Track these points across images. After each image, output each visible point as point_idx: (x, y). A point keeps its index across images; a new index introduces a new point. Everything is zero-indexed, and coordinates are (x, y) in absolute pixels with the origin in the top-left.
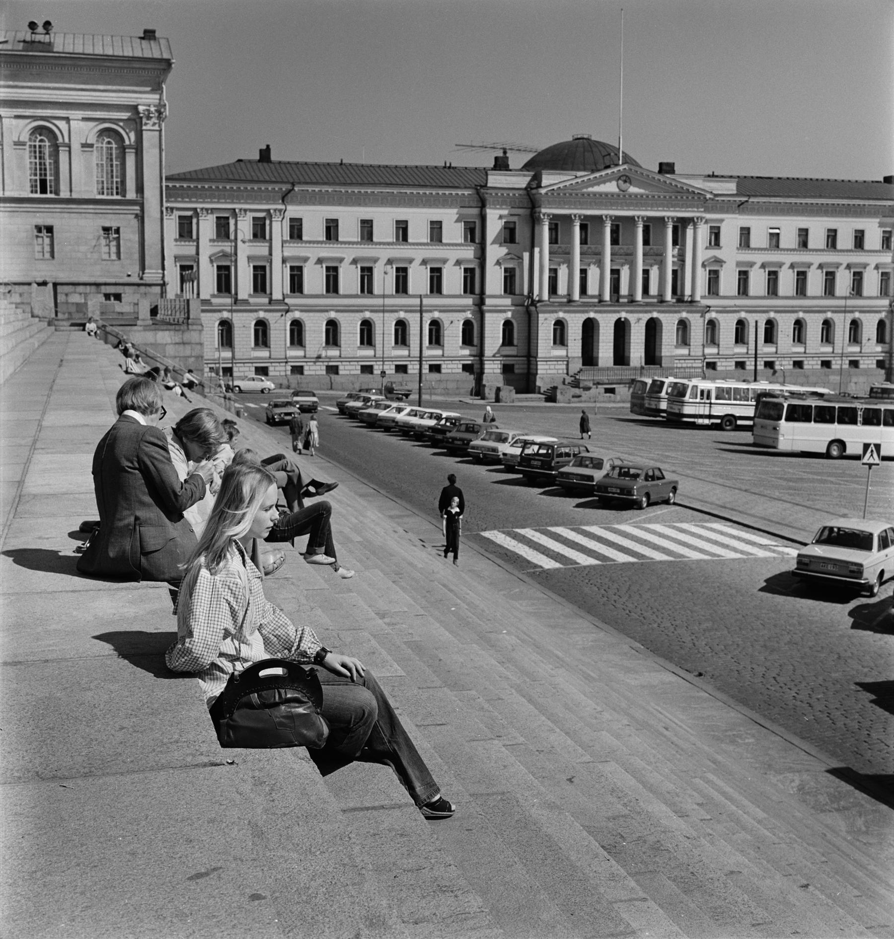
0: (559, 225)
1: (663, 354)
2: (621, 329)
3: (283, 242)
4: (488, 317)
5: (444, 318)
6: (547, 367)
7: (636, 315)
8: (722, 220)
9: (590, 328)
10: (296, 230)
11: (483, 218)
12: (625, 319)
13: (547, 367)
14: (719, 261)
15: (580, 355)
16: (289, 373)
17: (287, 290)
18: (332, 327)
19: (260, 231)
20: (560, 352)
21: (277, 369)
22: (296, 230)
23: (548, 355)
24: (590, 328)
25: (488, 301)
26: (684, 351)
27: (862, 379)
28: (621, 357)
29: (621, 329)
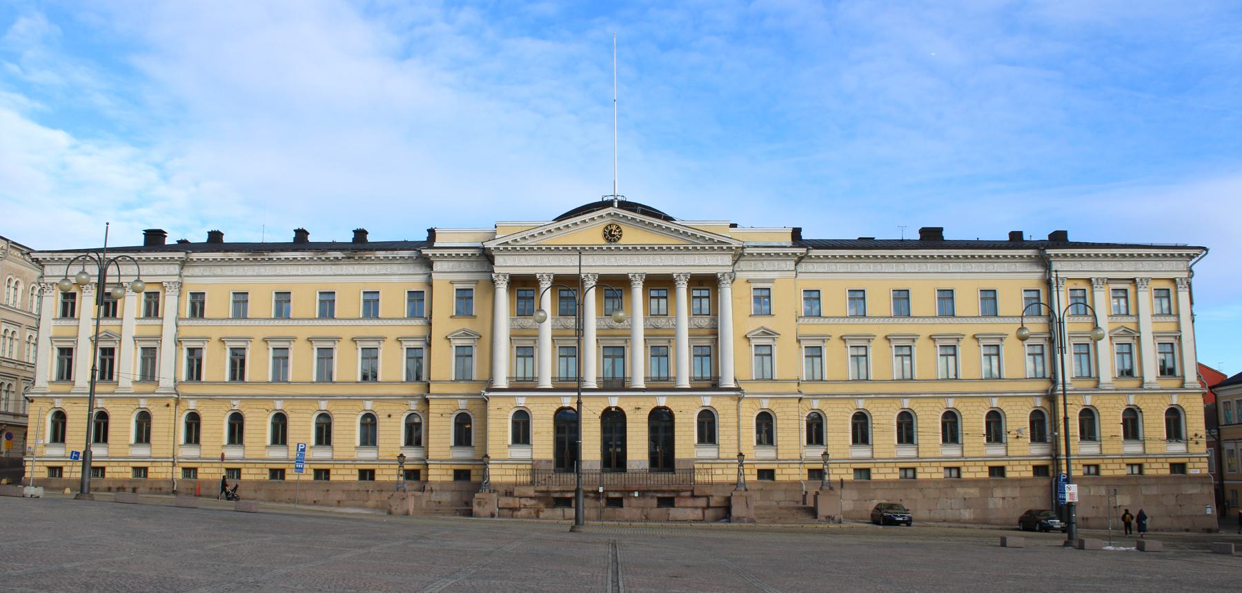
1: (677, 456)
2: (614, 422)
3: (178, 318)
5: (381, 411)
6: (503, 472)
7: (634, 403)
9: (567, 424)
10: (198, 306)
11: (430, 284)
12: (617, 408)
13: (503, 472)
14: (767, 333)
15: (551, 456)
17: (183, 376)
18: (280, 421)
19: (152, 307)
20: (521, 452)
21: (158, 470)
22: (198, 306)
23: (502, 457)
24: (567, 424)
25: (433, 389)
26: (708, 452)
27: (1009, 492)
29: (614, 422)
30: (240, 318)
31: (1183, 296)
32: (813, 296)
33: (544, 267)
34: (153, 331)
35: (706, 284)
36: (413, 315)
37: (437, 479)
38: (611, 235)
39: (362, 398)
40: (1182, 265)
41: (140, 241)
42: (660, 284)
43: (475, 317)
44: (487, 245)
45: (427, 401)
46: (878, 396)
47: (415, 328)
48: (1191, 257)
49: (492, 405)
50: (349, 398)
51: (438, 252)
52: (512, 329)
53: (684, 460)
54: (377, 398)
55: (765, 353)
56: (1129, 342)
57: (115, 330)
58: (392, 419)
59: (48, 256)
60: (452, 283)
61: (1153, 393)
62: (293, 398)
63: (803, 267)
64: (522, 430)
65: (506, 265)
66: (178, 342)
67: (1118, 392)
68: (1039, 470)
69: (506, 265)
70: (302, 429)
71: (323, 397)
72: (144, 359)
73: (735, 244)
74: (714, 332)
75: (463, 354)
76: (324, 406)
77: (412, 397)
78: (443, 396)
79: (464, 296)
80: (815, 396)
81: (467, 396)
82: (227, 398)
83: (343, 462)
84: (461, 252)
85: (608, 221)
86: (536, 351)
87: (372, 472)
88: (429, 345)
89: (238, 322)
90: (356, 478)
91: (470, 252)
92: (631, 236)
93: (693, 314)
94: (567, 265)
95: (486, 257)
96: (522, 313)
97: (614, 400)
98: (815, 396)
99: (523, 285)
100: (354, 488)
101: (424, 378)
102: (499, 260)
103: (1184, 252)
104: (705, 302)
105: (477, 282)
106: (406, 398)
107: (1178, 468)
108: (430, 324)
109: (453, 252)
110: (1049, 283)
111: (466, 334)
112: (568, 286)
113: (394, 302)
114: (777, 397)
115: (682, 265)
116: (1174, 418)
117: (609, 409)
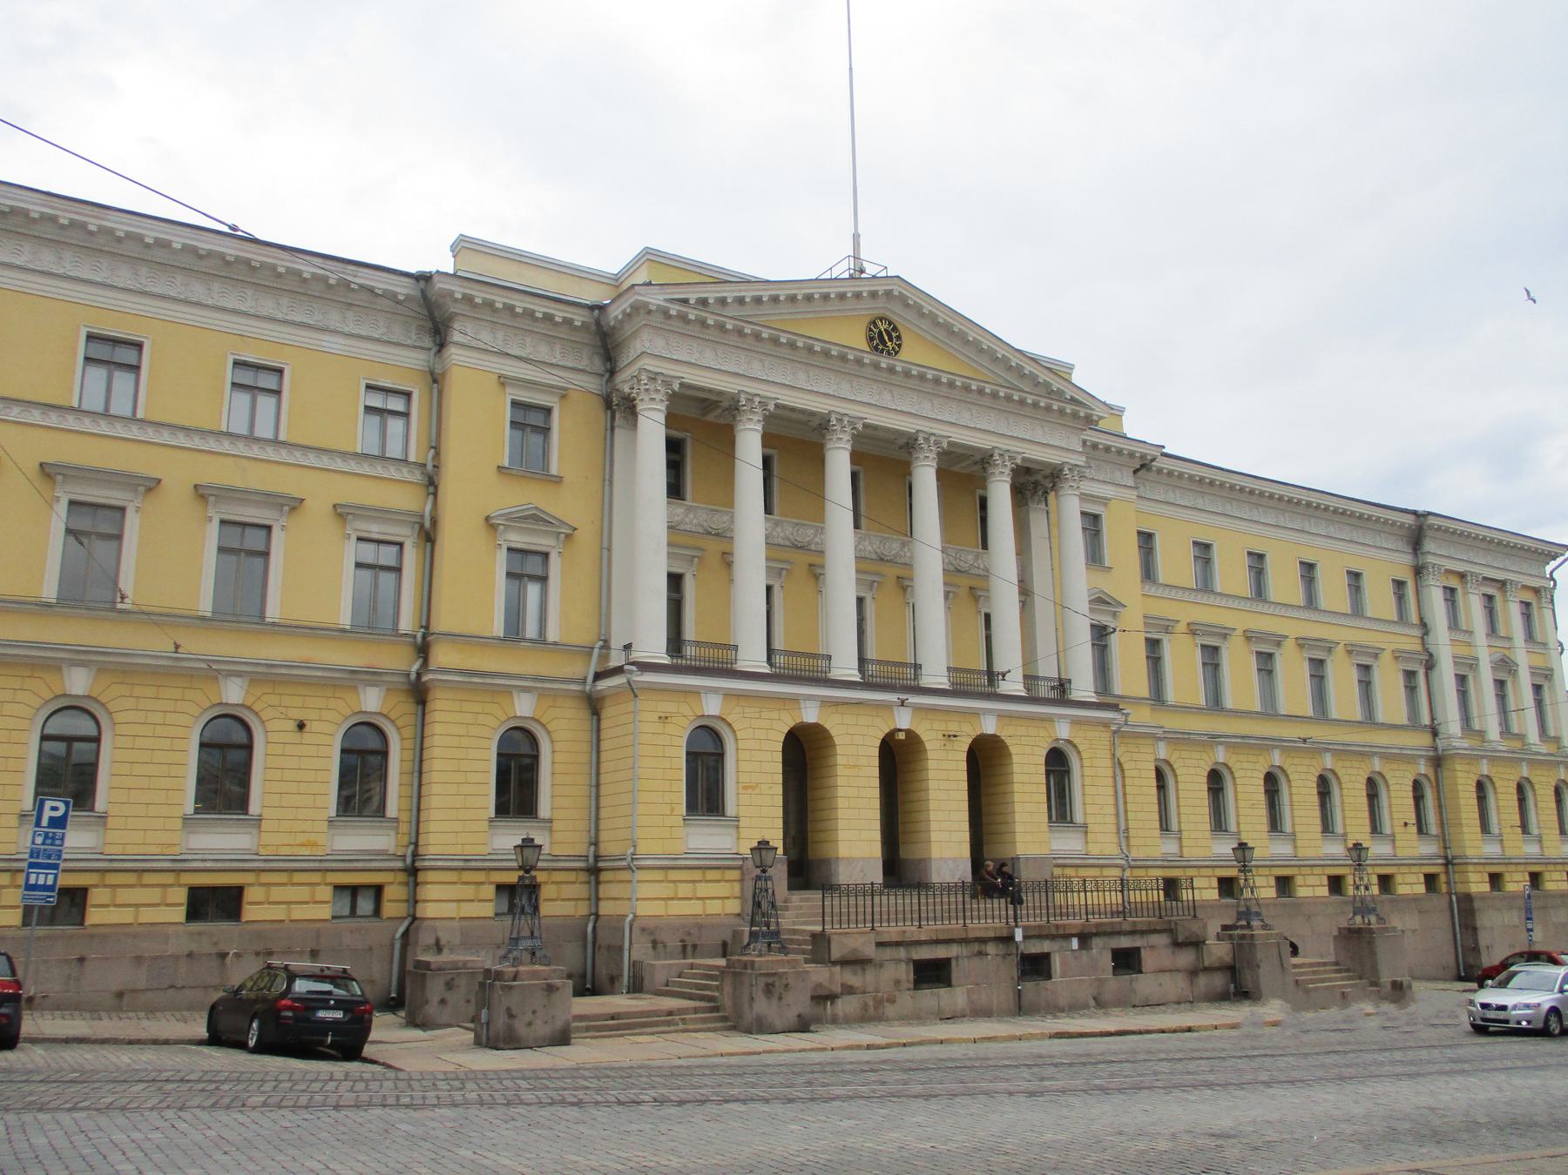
4: (442, 707)
12: (909, 732)
20: (709, 839)
25: (443, 656)
26: (1066, 843)
28: (899, 868)
33: (761, 383)
37: (449, 910)
39: (213, 672)
43: (558, 480)
45: (419, 694)
50: (175, 672)
53: (1038, 861)
54: (265, 676)
58: (307, 737)
60: (503, 381)
68: (1430, 880)
71: (81, 657)
77: (372, 676)
81: (540, 686)
87: (236, 893)
88: (428, 536)
90: (179, 914)
100: (186, 946)
105: (563, 394)
106: (355, 678)
108: (432, 484)
111: (536, 519)
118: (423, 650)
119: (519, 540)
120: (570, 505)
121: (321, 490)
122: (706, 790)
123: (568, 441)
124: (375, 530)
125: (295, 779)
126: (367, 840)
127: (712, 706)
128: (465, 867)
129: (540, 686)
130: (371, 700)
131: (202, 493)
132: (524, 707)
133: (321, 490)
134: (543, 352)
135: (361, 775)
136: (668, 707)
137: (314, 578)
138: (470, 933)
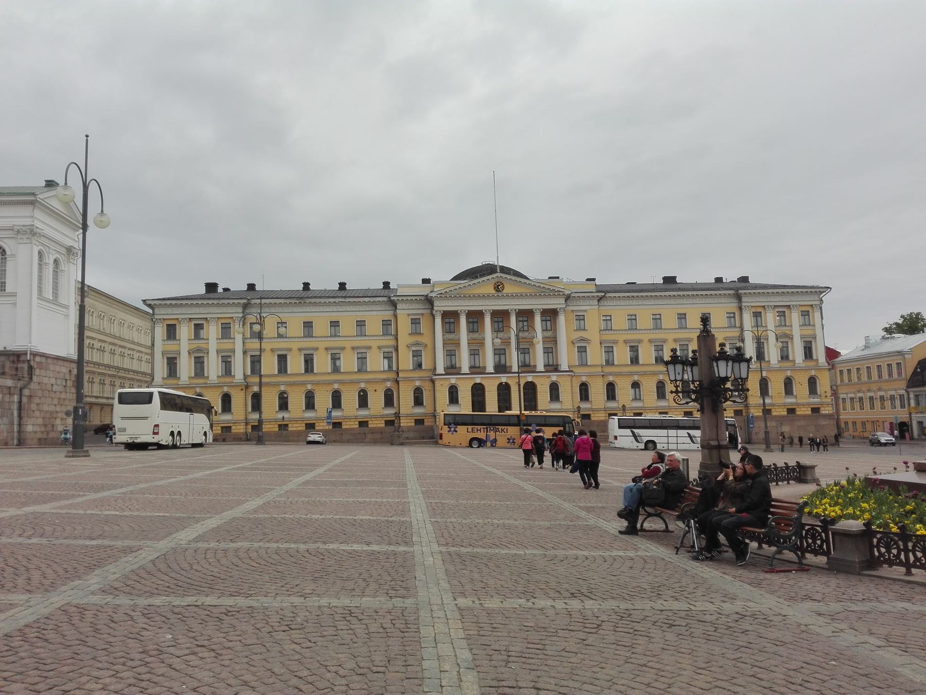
0: (450, 317)
2: (504, 391)
3: (244, 339)
8: (585, 311)
9: (478, 392)
11: (396, 316)
16: (250, 430)
24: (478, 392)
30: (226, 338)
31: (817, 315)
32: (608, 319)
33: (462, 306)
34: (175, 348)
35: (550, 315)
36: (386, 333)
38: (498, 287)
39: (359, 382)
40: (816, 298)
41: (203, 290)
42: (526, 315)
44: (431, 295)
45: (397, 382)
46: (645, 374)
47: (389, 341)
48: (821, 293)
49: (437, 384)
50: (352, 382)
51: (400, 298)
52: (444, 340)
54: (367, 381)
55: (582, 350)
56: (785, 340)
57: (204, 346)
59: (160, 302)
60: (409, 315)
61: (801, 369)
62: (318, 383)
63: (602, 303)
64: (453, 397)
65: (441, 306)
66: (245, 353)
67: (780, 370)
69: (441, 306)
70: (323, 401)
71: (336, 382)
72: (279, 362)
73: (567, 292)
74: (554, 340)
75: (417, 354)
76: (336, 386)
77: (388, 380)
78: (407, 379)
79: (415, 322)
80: (611, 374)
81: (420, 379)
82: (277, 384)
83: (349, 418)
84: (414, 298)
85: (497, 280)
86: (507, 351)
88: (397, 350)
89: (225, 341)
91: (418, 298)
92: (508, 289)
93: (544, 330)
94: (475, 305)
95: (429, 301)
96: (450, 332)
97: (504, 379)
98: (611, 374)
99: (450, 317)
101: (394, 369)
102: (436, 303)
103: (818, 290)
104: (549, 323)
105: (423, 314)
106: (385, 380)
107: (816, 410)
108: (397, 339)
109: (409, 298)
110: (740, 309)
111: (417, 344)
112: (475, 317)
113: (374, 326)
114: (590, 375)
115: (537, 304)
116: (812, 382)
117: (501, 383)
118: (398, 373)
119: (414, 348)
120: (425, 339)
121: (375, 344)
122: (453, 397)
123: (424, 326)
124: (386, 350)
125: (376, 400)
126: (390, 411)
127: (453, 381)
128: (408, 416)
129: (420, 379)
130: (389, 384)
131: (353, 348)
132: (418, 383)
133: (375, 344)
134: (417, 306)
135: (389, 399)
136: (442, 382)
137: (376, 362)
138: (409, 429)
